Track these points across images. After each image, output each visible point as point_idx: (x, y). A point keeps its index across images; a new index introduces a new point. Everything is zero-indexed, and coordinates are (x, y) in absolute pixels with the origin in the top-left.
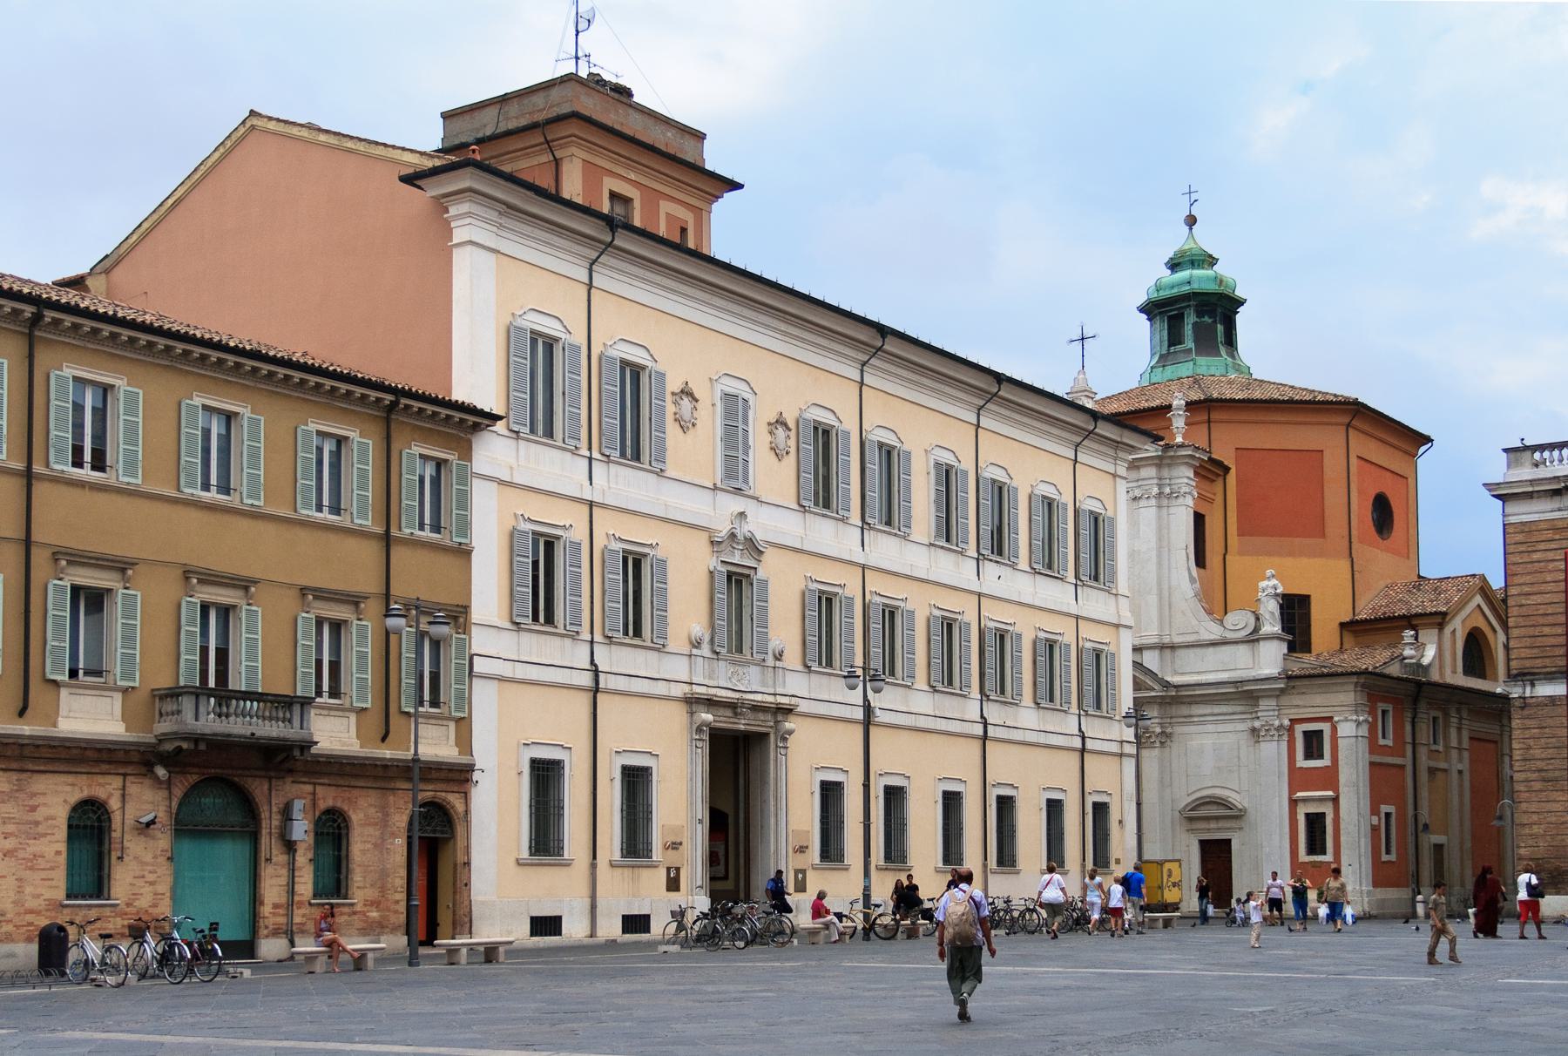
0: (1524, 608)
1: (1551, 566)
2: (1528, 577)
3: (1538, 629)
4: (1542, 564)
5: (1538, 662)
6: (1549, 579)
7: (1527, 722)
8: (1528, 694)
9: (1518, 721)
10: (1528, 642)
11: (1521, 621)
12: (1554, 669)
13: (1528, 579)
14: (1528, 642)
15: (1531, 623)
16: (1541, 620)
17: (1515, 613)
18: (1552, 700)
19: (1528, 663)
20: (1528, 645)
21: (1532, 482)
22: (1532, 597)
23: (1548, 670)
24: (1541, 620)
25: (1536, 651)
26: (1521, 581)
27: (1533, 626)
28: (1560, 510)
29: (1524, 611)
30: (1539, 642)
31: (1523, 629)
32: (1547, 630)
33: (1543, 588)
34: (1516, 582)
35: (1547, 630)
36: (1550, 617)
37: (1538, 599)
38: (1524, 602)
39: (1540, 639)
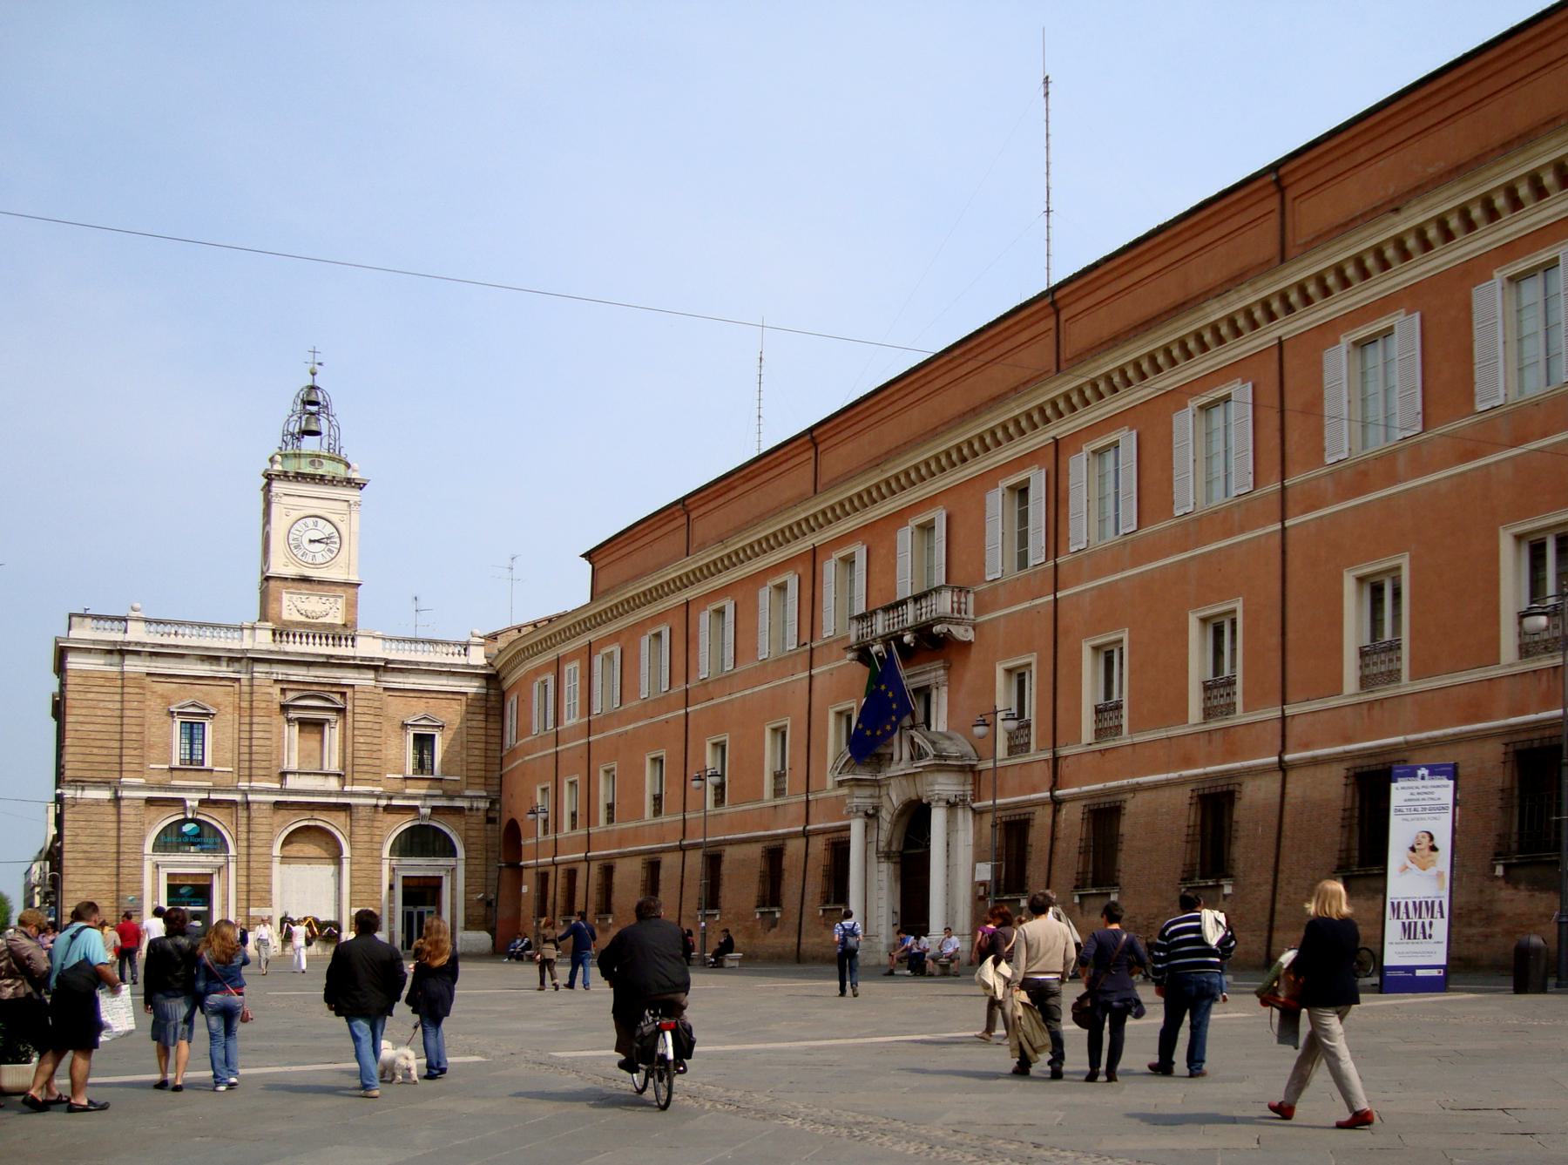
1: (102, 704)
3: (90, 749)
11: (76, 742)
13: (84, 712)
14: (80, 758)
18: (97, 802)
21: (94, 642)
22: (87, 726)
28: (111, 665)
29: (78, 735)
30: (89, 758)
32: (95, 751)
33: (94, 719)
35: (95, 751)
37: (91, 727)
38: (79, 728)
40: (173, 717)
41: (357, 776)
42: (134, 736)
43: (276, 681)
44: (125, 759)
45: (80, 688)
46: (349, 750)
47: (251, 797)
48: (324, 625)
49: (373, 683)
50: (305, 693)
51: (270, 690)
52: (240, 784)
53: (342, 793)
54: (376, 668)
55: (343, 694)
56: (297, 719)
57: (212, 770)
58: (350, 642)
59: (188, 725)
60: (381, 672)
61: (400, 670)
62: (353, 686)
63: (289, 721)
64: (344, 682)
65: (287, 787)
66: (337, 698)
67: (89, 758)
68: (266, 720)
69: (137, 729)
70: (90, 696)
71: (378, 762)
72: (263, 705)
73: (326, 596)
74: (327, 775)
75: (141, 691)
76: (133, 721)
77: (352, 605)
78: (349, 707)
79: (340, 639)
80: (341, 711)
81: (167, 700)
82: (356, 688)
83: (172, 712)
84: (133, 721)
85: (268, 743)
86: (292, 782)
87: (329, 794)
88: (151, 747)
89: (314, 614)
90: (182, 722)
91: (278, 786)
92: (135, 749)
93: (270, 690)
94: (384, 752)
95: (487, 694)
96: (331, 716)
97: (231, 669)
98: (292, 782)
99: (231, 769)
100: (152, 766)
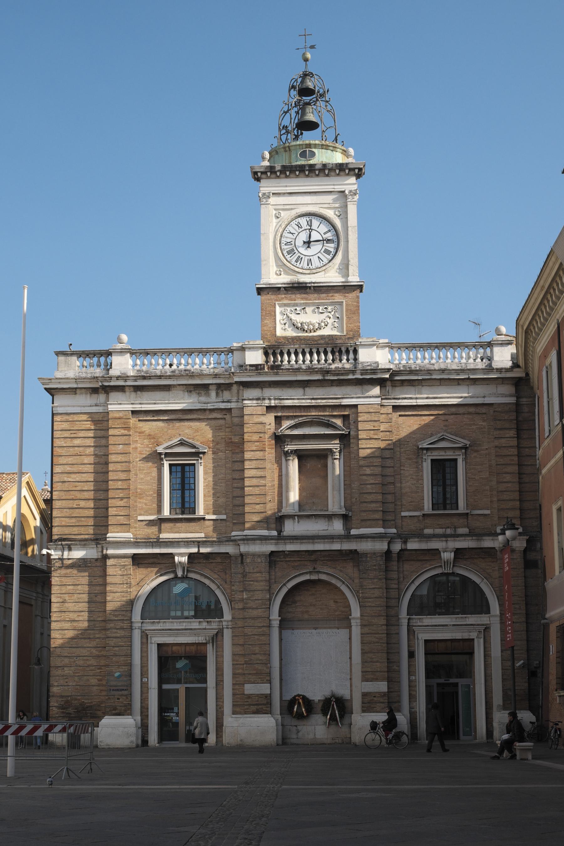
0: (67, 484)
2: (70, 459)
3: (76, 502)
4: (81, 449)
5: (75, 530)
6: (86, 462)
7: (63, 579)
8: (65, 556)
9: (57, 579)
10: (67, 512)
11: (63, 495)
12: (87, 537)
13: (70, 460)
15: (71, 497)
16: (79, 495)
17: (59, 488)
19: (66, 531)
20: (67, 515)
22: (73, 476)
23: (83, 537)
24: (79, 495)
25: (74, 520)
26: (65, 462)
27: (73, 499)
29: (66, 486)
30: (76, 513)
31: (64, 502)
34: (61, 462)
36: (86, 493)
37: (77, 477)
38: (66, 479)
39: (77, 510)
40: (162, 459)
41: (364, 515)
42: (119, 484)
43: (269, 408)
44: (111, 511)
45: (67, 434)
46: (355, 485)
47: (244, 548)
48: (322, 337)
49: (378, 400)
50: (301, 420)
51: (262, 419)
52: (234, 533)
53: (348, 537)
54: (381, 382)
55: (345, 418)
56: (296, 451)
57: (204, 519)
58: (351, 356)
59: (179, 469)
60: (389, 388)
61: (411, 383)
62: (356, 406)
63: (287, 454)
64: (346, 402)
65: (285, 534)
66: (339, 422)
67: (76, 513)
68: (259, 454)
69: (123, 476)
70: (77, 442)
71: (390, 498)
72: (255, 437)
73: (323, 304)
74: (330, 517)
75: (126, 432)
76: (119, 467)
77: (354, 311)
78: (352, 433)
79: (340, 352)
80: (345, 439)
81: (154, 439)
82: (360, 408)
83: (160, 454)
84: (119, 467)
85: (262, 482)
86: (290, 528)
87: (331, 538)
88: (140, 495)
89: (312, 327)
90: (171, 465)
91: (275, 533)
92: (122, 499)
93: (262, 419)
94: (398, 485)
95: (517, 404)
96: (335, 445)
97: (220, 399)
98: (290, 528)
99: (224, 517)
100: (140, 518)
